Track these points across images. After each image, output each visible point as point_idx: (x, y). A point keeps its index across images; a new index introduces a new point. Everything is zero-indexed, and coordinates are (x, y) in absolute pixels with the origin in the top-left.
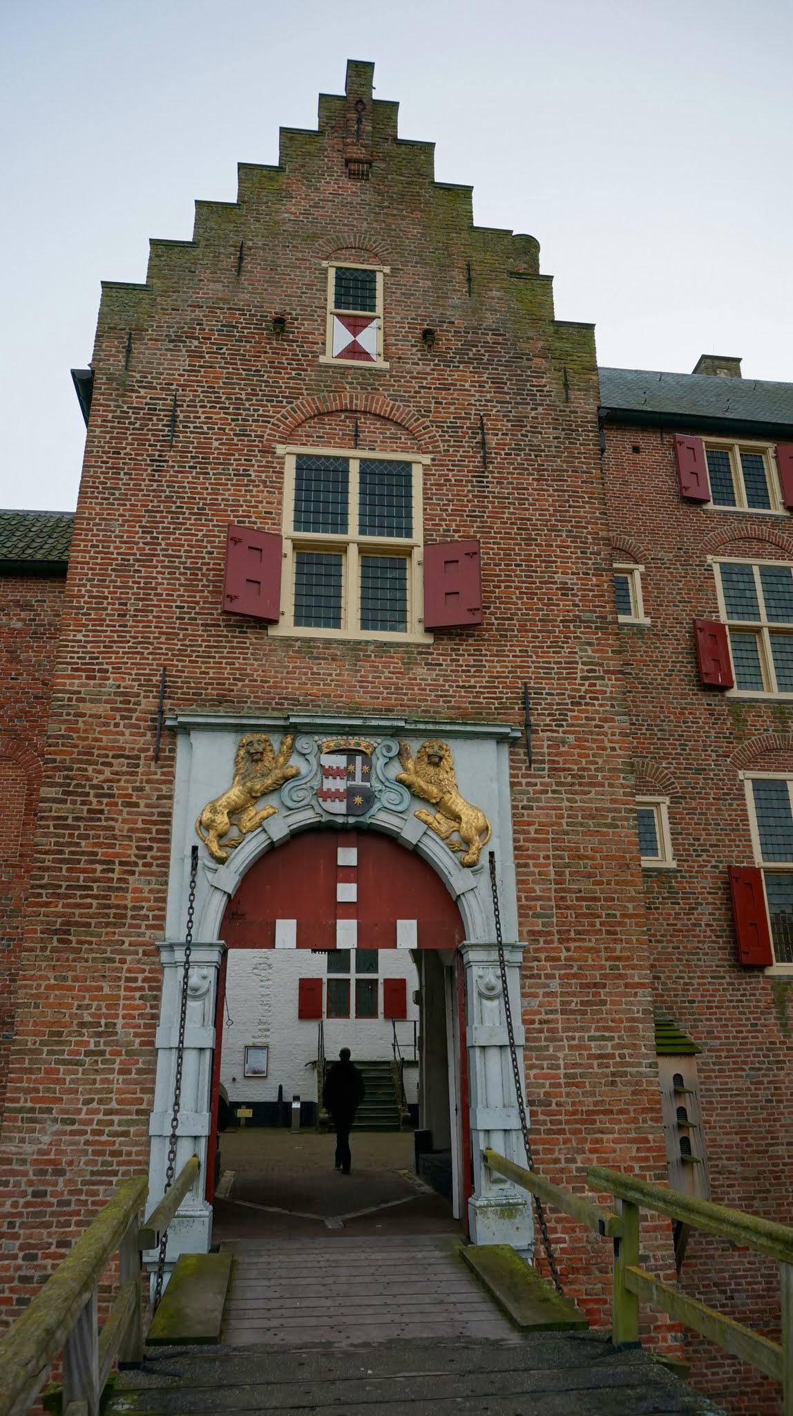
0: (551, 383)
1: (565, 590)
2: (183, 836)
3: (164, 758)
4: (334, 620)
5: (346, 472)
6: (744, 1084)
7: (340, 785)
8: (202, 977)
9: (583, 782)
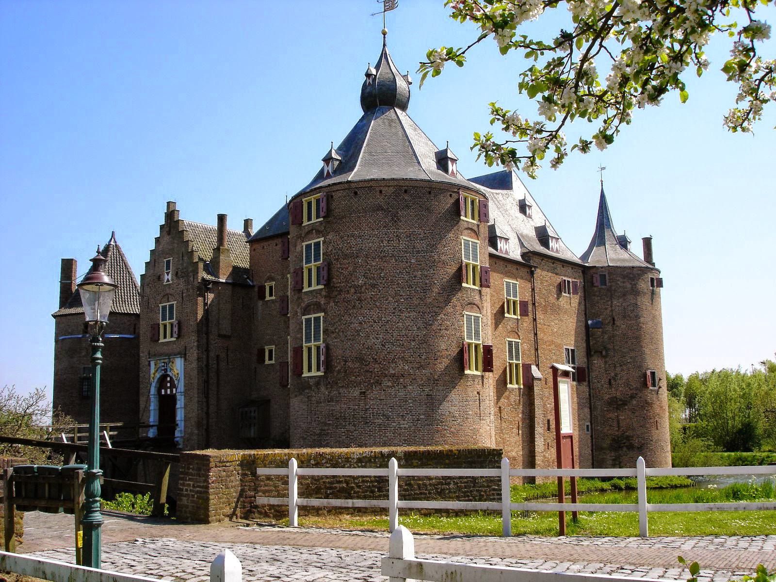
6: (282, 412)
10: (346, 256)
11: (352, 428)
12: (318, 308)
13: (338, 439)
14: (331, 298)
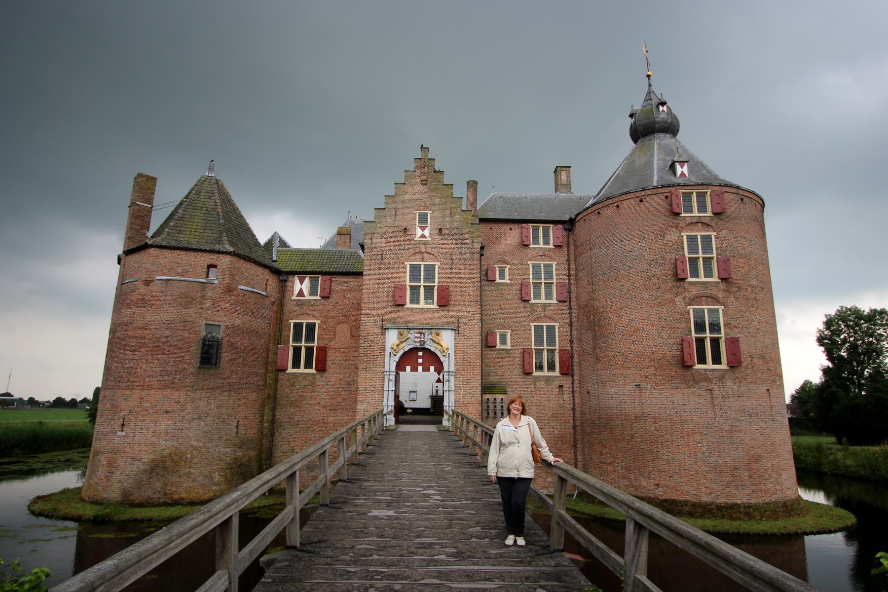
0: (469, 241)
1: (469, 294)
2: (388, 350)
3: (383, 334)
4: (418, 303)
5: (421, 268)
7: (418, 340)
8: (393, 377)
9: (470, 338)
10: (741, 256)
11: (765, 426)
12: (715, 300)
13: (754, 436)
14: (730, 293)
